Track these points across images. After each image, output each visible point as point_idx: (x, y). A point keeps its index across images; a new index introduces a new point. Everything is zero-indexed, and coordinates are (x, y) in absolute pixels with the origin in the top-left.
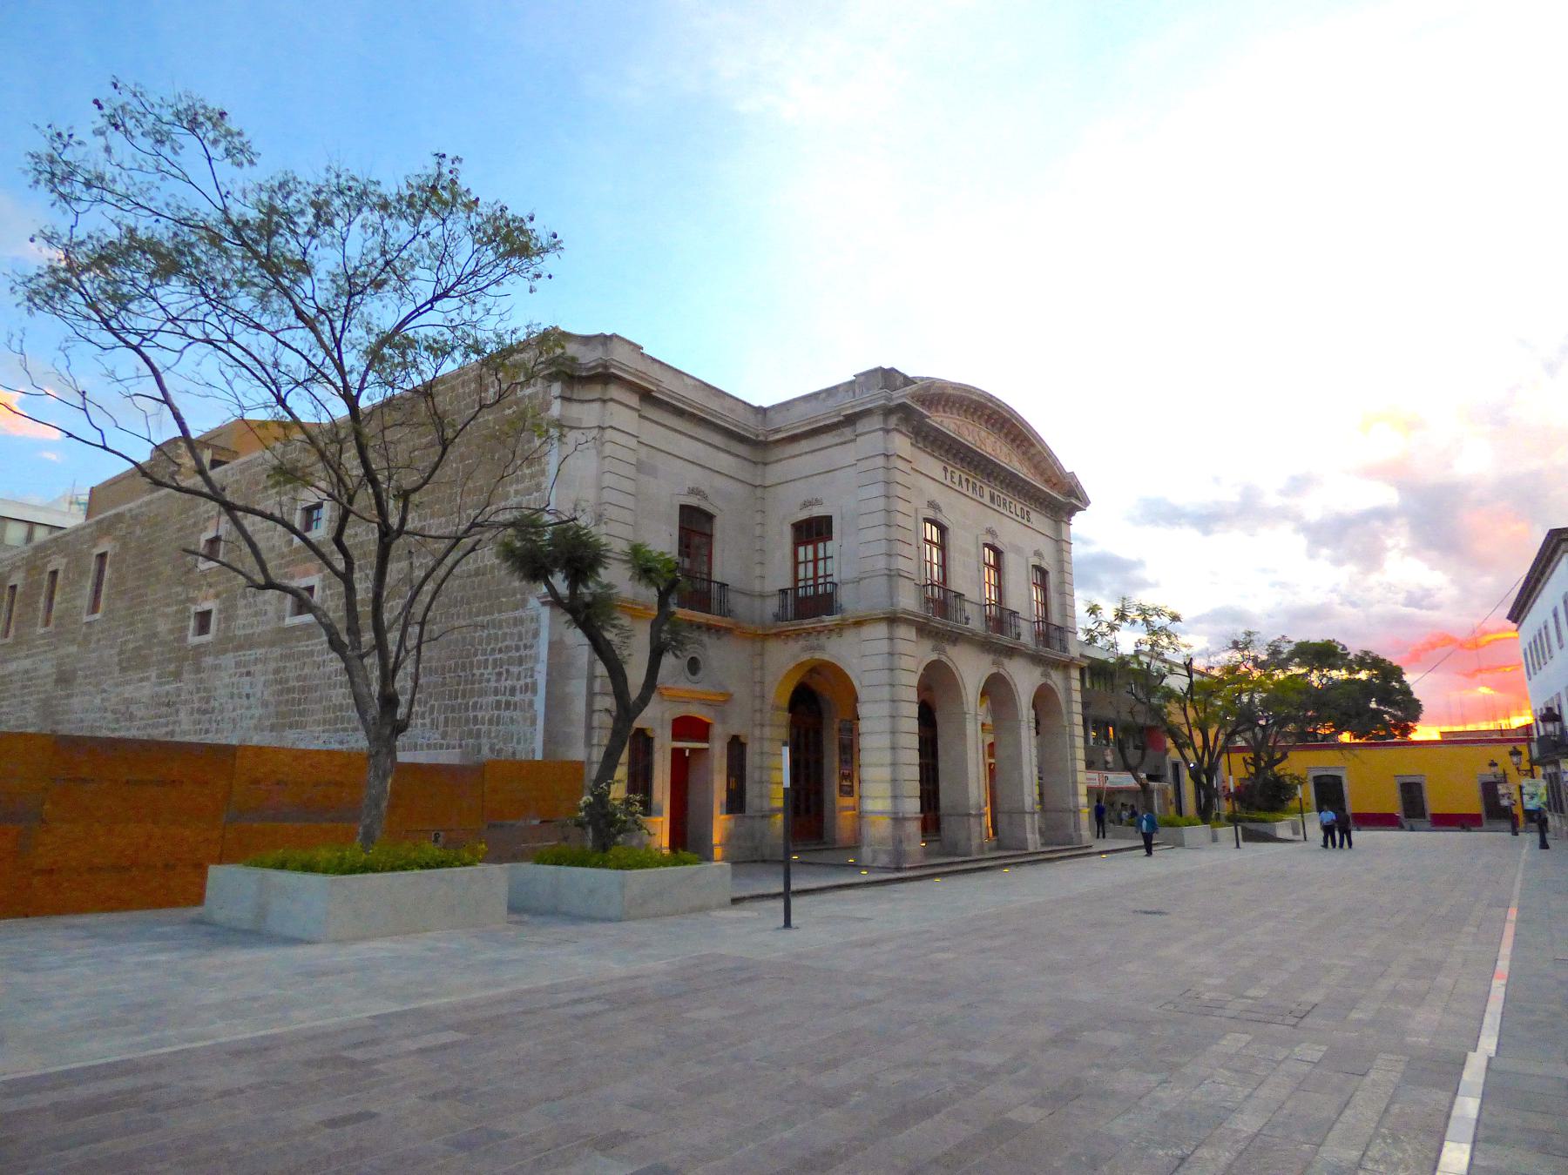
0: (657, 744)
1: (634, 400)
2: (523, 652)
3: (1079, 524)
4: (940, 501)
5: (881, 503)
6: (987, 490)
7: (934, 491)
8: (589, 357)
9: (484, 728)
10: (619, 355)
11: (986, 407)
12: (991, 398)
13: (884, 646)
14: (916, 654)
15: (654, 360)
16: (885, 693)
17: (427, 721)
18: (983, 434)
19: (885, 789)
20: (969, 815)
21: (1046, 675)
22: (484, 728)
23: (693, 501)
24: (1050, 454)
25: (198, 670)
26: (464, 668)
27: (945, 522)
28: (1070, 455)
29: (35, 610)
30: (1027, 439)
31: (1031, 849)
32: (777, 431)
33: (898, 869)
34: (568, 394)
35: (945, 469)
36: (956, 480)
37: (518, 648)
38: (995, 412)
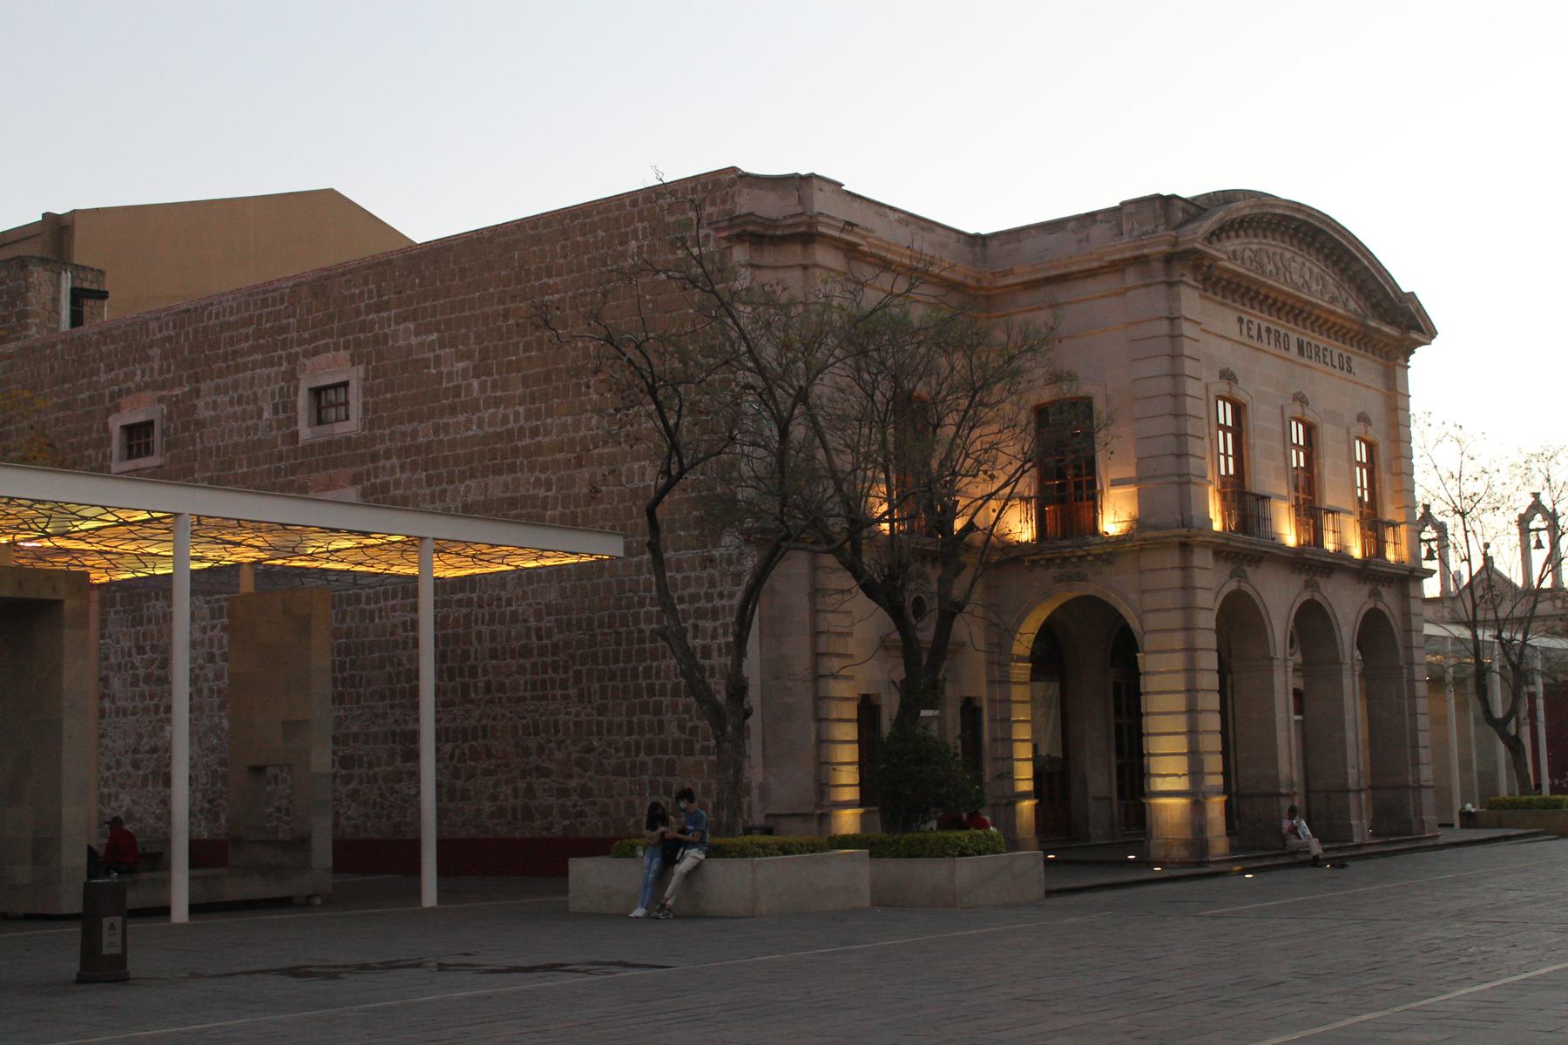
2: (717, 603)
3: (1422, 366)
4: (1237, 368)
5: (1166, 384)
6: (1293, 338)
7: (1225, 354)
8: (771, 206)
9: (667, 700)
10: (821, 203)
11: (1293, 219)
12: (1299, 207)
13: (1174, 578)
14: (1211, 584)
16: (1178, 640)
17: (572, 691)
18: (1288, 255)
19: (1180, 765)
20: (1348, 791)
21: (1374, 594)
22: (667, 700)
25: (138, 622)
26: (624, 623)
27: (1241, 396)
28: (1407, 271)
29: (440, 623)
30: (1347, 251)
31: (1357, 840)
32: (1005, 274)
33: (1199, 864)
34: (757, 261)
35: (1240, 320)
36: (1254, 333)
37: (709, 597)
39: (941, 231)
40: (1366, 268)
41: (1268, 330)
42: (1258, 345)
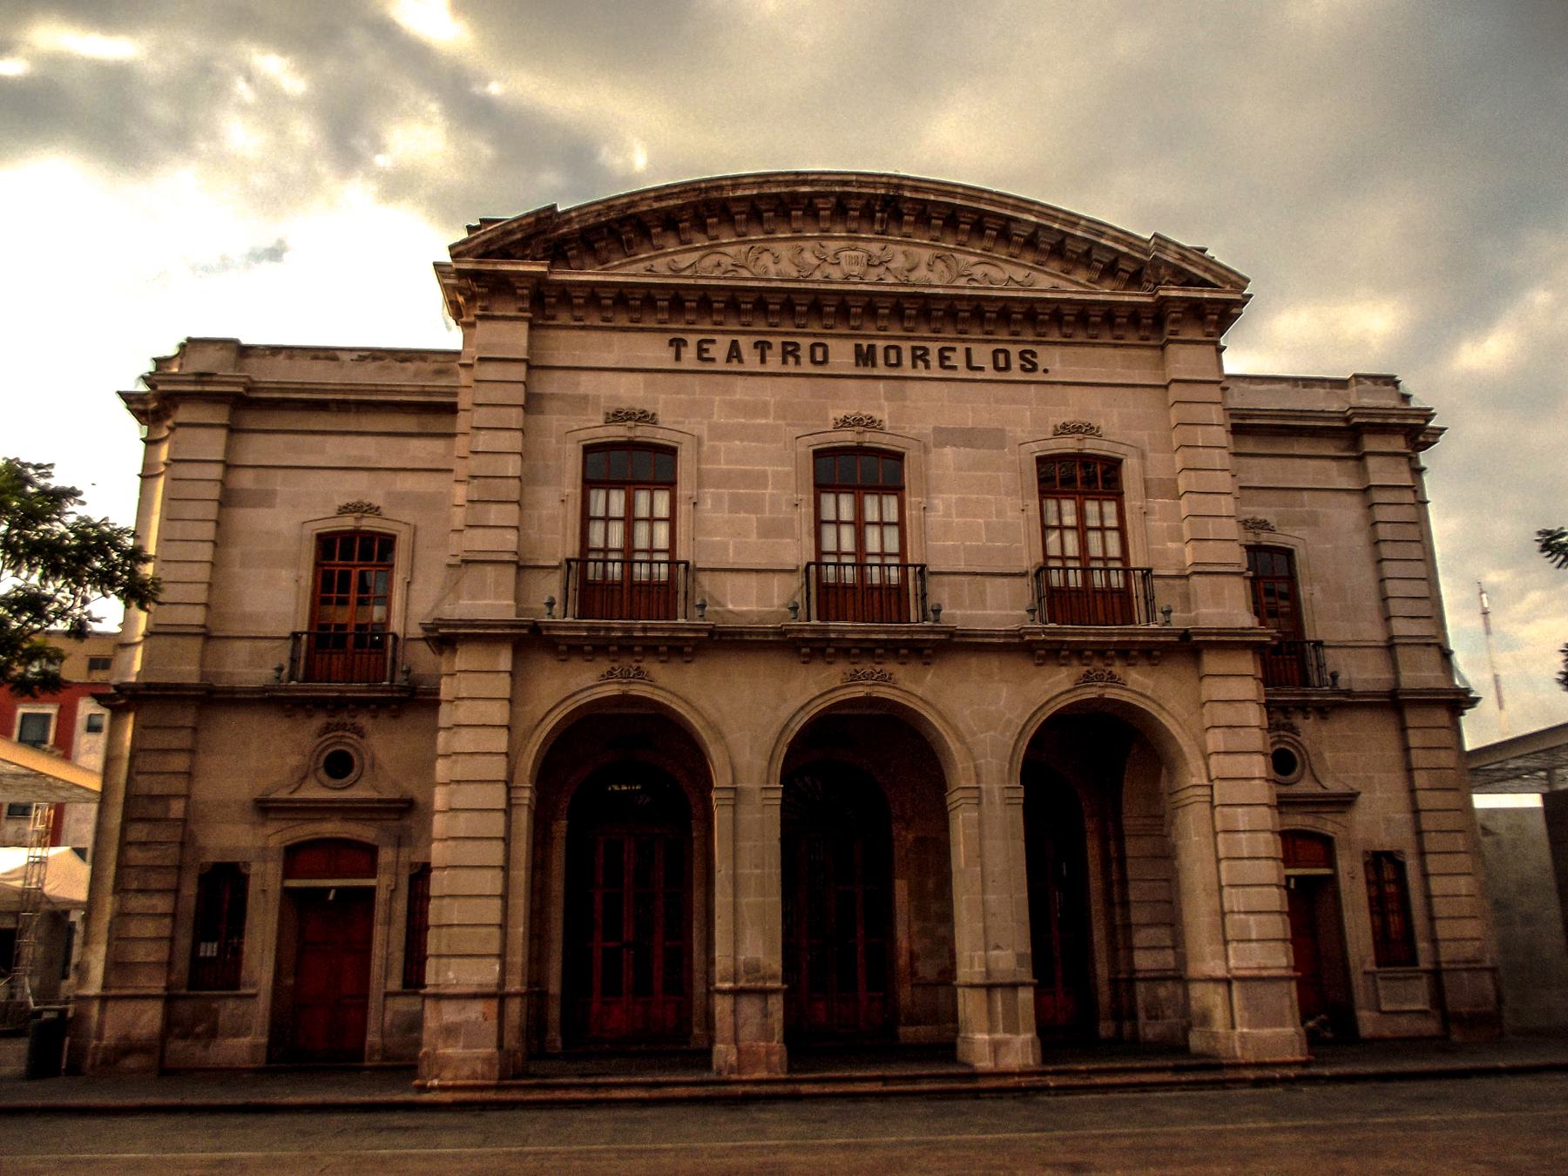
0: (254, 886)
1: (220, 415)
7: (630, 391)
15: (275, 350)
18: (832, 246)
23: (348, 523)
24: (1073, 219)
35: (678, 344)
38: (842, 198)
39: (440, 358)
40: (1038, 226)
41: (762, 347)
42: (735, 366)
